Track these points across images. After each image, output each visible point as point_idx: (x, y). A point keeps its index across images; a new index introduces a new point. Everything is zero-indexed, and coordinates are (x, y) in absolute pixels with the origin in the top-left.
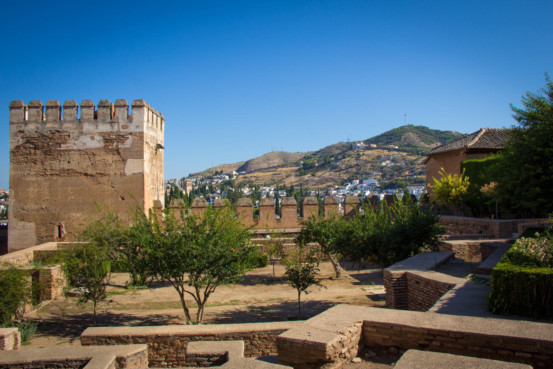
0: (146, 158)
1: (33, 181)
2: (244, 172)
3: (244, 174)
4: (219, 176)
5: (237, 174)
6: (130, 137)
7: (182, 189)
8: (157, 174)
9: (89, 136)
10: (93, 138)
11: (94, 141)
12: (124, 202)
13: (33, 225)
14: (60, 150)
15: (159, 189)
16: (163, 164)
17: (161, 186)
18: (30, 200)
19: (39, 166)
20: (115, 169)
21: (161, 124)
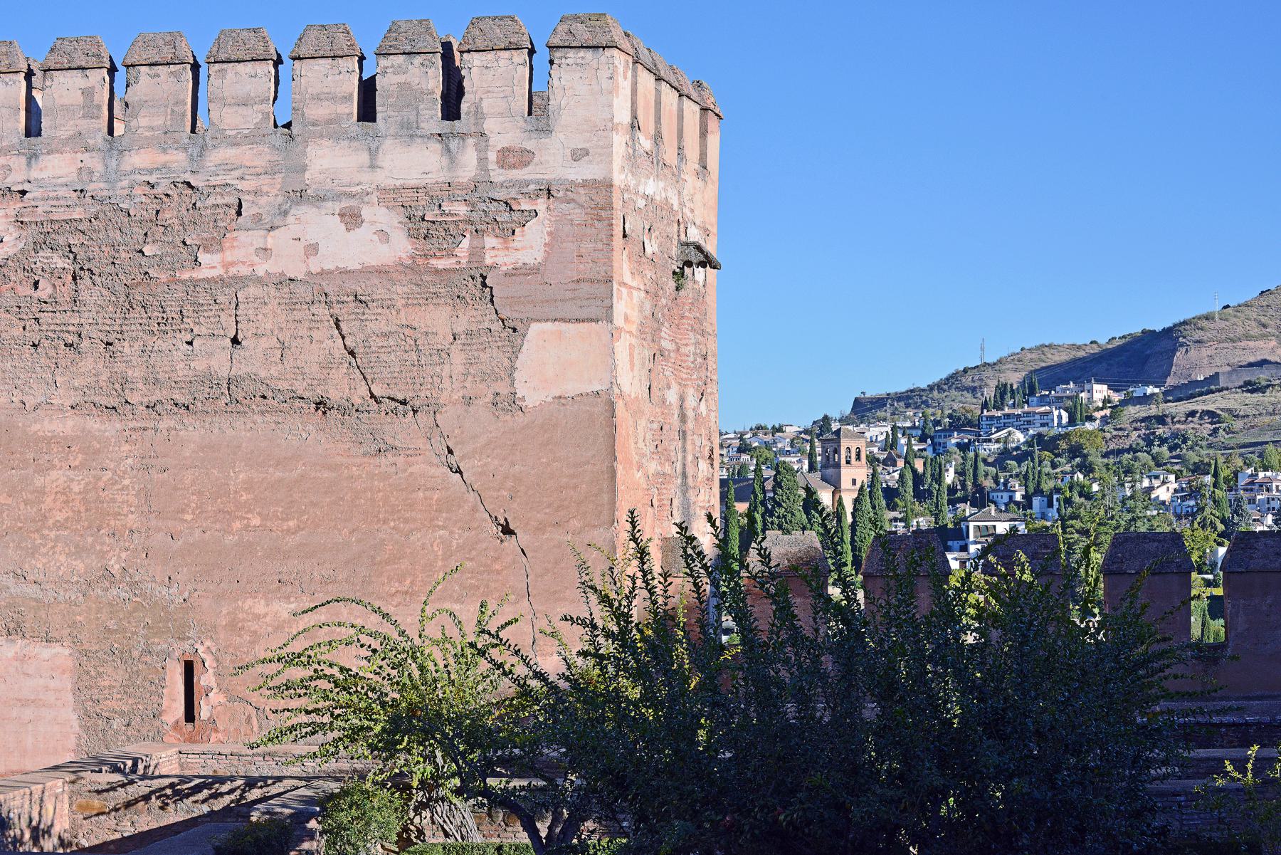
0: (626, 319)
1: (65, 438)
2: (1150, 390)
3: (1145, 400)
4: (999, 414)
5: (1116, 397)
6: (541, 205)
7: (815, 479)
8: (682, 399)
9: (338, 207)
10: (352, 219)
11: (364, 232)
12: (510, 542)
13: (61, 653)
14: (195, 283)
15: (690, 481)
16: (712, 346)
17: (704, 465)
18: (53, 535)
19: (90, 363)
20: (466, 375)
21: (704, 133)
